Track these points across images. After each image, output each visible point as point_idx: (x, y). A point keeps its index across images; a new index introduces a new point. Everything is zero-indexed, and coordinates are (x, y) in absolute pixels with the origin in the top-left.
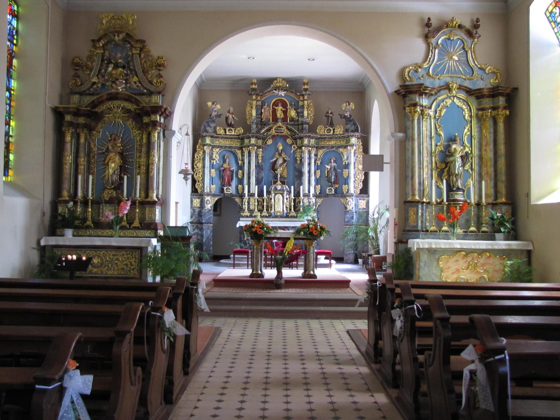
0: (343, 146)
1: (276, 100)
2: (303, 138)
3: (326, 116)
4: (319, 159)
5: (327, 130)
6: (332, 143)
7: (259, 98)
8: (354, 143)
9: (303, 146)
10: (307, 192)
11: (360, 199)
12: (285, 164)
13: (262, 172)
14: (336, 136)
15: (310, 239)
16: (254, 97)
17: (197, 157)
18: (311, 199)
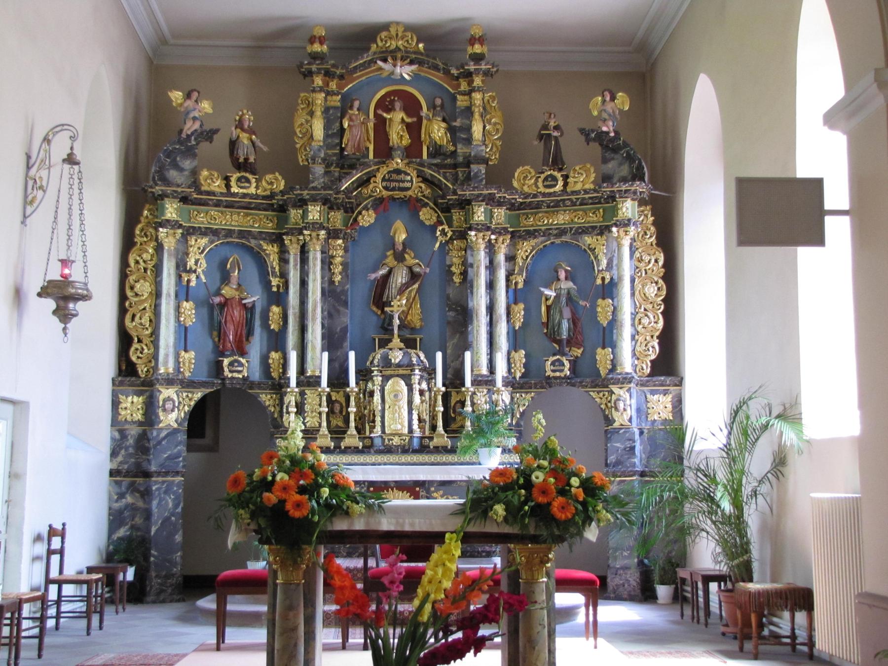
0: (594, 228)
1: (388, 94)
2: (469, 202)
3: (541, 137)
4: (521, 270)
5: (546, 179)
6: (561, 219)
7: (333, 85)
8: (630, 216)
9: (470, 229)
10: (484, 371)
11: (653, 393)
12: (416, 286)
13: (342, 309)
14: (573, 197)
15: (535, 539)
16: (318, 81)
17: (137, 262)
18: (498, 391)
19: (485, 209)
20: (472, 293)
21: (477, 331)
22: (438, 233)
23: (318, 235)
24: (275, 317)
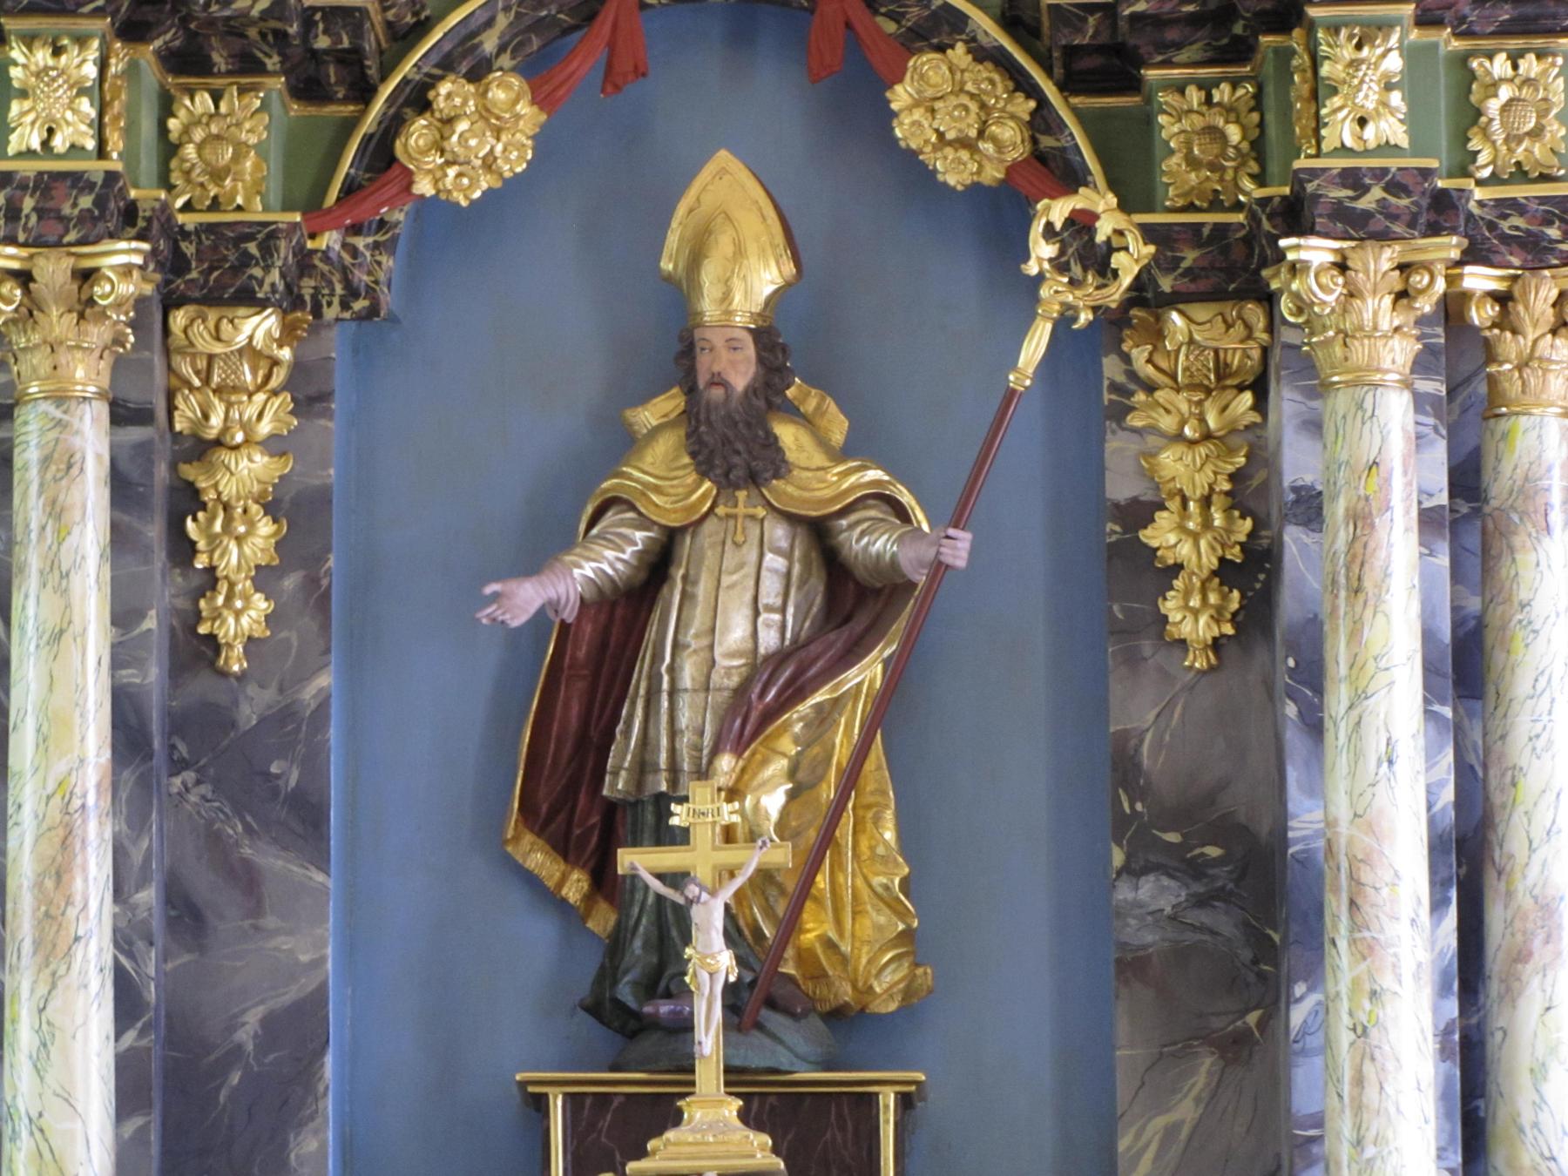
12: (868, 673)
13: (273, 861)
19: (1412, 54)
20: (1315, 726)
21: (1360, 1031)
22: (1042, 251)
23: (86, 276)
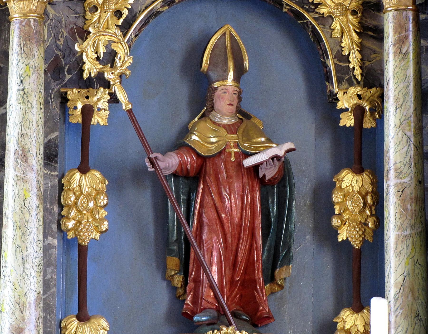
24: (349, 204)
